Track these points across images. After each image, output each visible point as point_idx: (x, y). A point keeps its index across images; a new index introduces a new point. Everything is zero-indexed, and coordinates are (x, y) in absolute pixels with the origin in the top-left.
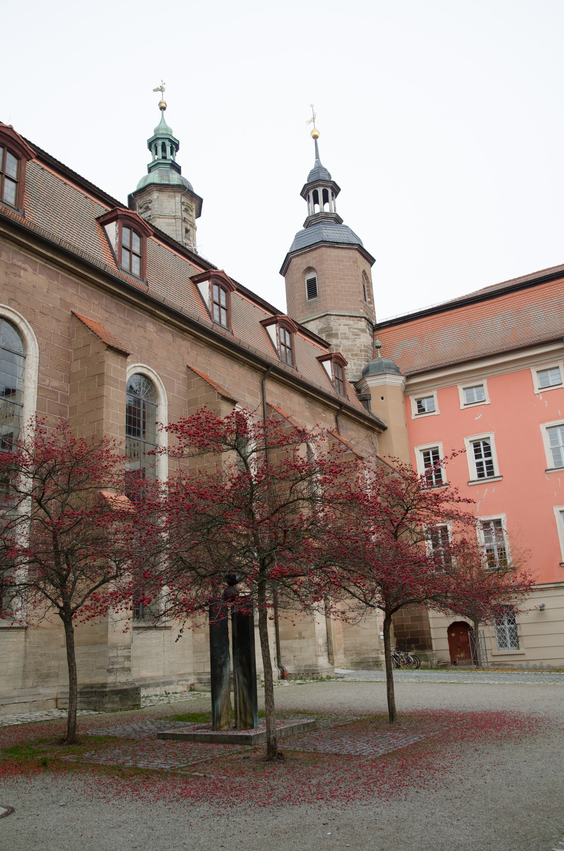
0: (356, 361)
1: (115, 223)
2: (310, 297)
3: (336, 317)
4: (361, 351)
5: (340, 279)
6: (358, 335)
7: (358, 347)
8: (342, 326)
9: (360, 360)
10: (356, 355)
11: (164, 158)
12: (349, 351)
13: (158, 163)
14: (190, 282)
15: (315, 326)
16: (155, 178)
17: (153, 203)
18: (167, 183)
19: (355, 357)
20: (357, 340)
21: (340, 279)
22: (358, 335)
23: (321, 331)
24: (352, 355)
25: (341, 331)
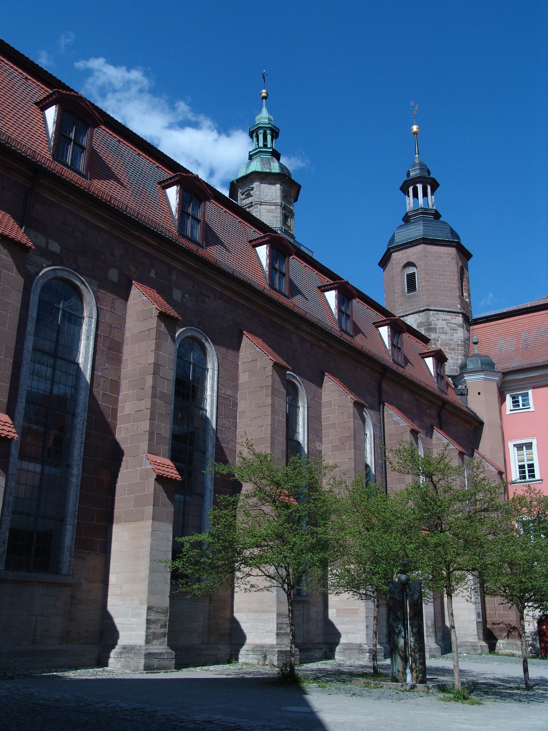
0: (453, 355)
1: (266, 245)
2: (409, 291)
3: (434, 312)
4: (458, 345)
5: (440, 275)
6: (456, 330)
7: (456, 342)
8: (440, 321)
9: (457, 354)
10: (453, 349)
11: (265, 146)
12: (447, 345)
13: (260, 151)
14: (316, 289)
15: (414, 319)
16: (256, 166)
17: (254, 190)
18: (268, 171)
19: (452, 352)
20: (454, 334)
21: (440, 275)
22: (456, 330)
23: (420, 325)
24: (449, 349)
25: (439, 326)
